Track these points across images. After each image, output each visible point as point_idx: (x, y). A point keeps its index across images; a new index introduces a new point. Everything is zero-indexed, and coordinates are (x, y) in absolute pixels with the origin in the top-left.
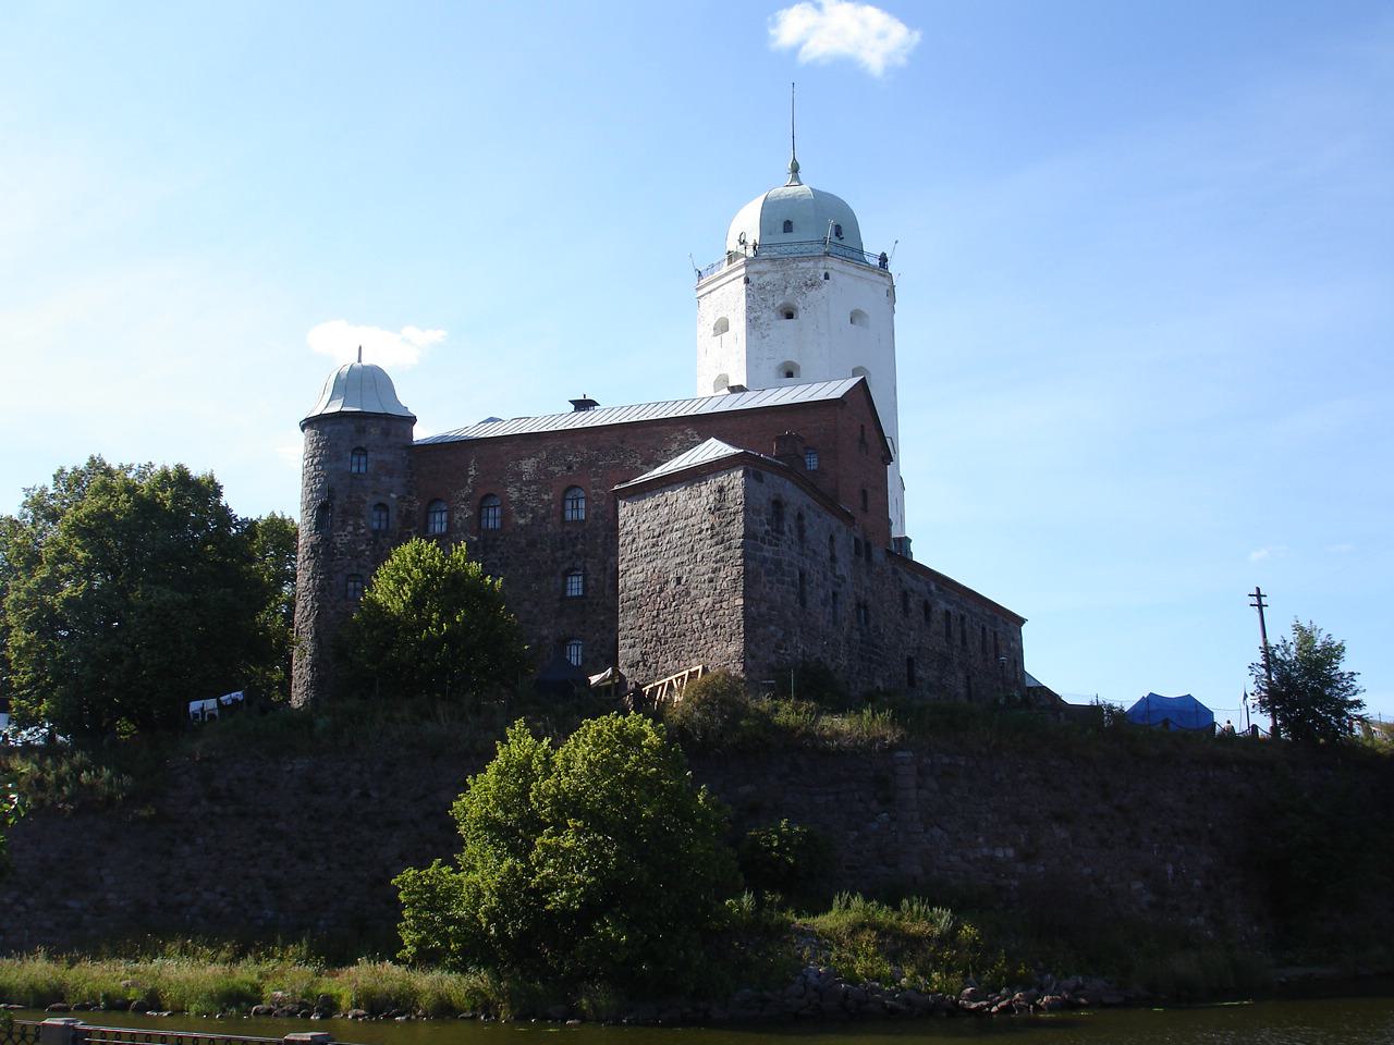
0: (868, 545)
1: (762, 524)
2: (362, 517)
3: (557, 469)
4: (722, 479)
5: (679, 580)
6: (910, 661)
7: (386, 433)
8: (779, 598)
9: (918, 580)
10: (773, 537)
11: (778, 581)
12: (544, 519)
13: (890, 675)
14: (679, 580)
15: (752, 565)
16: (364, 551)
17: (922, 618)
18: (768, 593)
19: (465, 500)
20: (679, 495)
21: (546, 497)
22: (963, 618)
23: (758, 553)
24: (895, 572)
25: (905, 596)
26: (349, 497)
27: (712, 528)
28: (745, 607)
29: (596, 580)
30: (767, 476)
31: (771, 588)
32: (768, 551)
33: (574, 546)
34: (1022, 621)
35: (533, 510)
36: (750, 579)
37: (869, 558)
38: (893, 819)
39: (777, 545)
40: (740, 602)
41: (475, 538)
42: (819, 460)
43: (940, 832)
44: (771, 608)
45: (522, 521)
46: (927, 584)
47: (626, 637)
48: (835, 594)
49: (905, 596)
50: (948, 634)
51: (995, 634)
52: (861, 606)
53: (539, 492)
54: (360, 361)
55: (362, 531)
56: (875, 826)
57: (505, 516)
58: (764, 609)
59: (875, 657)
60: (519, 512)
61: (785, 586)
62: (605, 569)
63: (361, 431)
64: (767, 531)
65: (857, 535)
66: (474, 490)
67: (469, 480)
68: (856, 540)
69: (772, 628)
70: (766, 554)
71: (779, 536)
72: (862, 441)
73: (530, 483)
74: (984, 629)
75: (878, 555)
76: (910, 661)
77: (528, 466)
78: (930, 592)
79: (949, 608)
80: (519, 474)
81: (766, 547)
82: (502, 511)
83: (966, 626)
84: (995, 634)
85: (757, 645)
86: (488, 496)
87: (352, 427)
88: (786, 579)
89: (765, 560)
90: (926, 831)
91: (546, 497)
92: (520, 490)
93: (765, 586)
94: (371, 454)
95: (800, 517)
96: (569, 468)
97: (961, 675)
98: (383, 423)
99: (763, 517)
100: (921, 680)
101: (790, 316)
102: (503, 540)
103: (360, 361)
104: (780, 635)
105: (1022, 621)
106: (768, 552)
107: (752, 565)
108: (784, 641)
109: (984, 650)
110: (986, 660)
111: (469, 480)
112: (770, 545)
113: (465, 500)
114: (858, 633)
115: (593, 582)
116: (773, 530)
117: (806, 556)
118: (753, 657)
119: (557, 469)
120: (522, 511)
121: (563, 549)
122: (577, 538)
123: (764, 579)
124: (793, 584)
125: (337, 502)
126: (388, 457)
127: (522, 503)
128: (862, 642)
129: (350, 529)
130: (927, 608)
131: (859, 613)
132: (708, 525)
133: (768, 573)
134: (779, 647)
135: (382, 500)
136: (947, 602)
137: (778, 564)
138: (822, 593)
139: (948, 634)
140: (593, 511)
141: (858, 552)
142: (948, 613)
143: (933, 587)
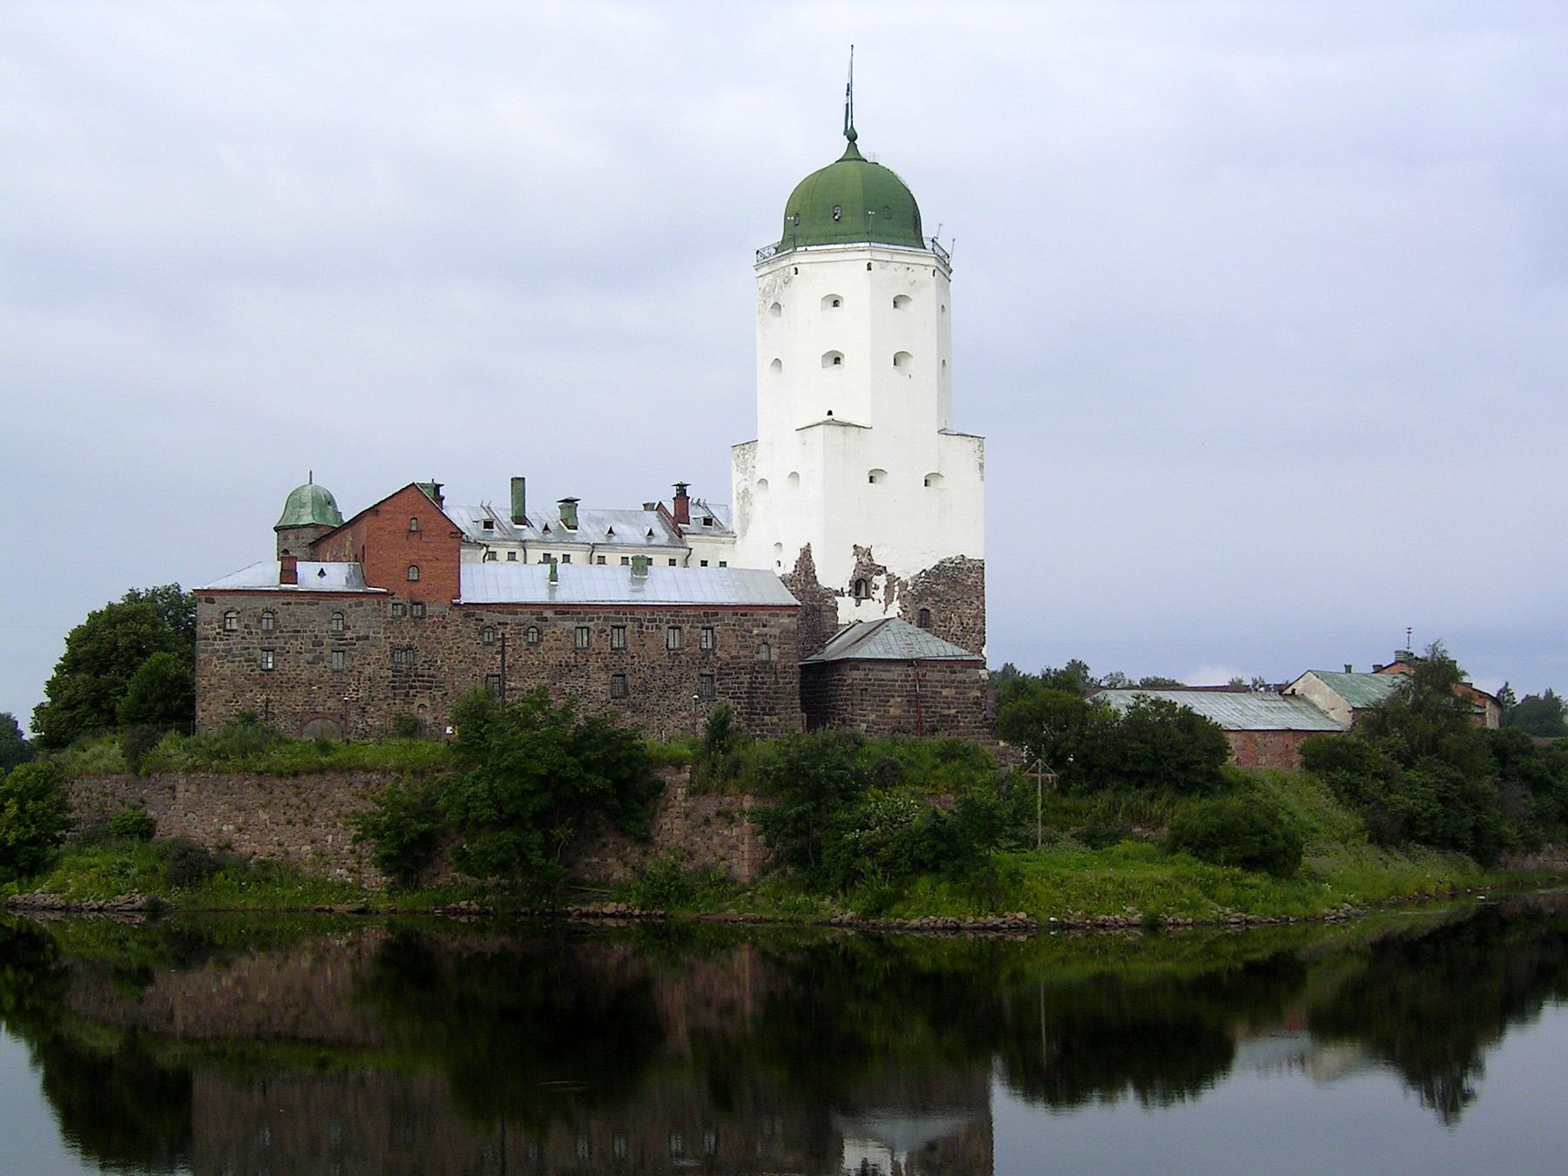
1: (215, 629)
8: (228, 672)
10: (224, 635)
11: (228, 661)
13: (446, 694)
18: (218, 671)
23: (209, 648)
32: (220, 645)
39: (227, 640)
43: (194, 815)
54: (311, 483)
59: (417, 684)
61: (237, 663)
63: (286, 539)
64: (218, 634)
69: (221, 691)
70: (218, 647)
71: (230, 633)
78: (545, 619)
79: (591, 625)
81: (218, 642)
83: (627, 633)
88: (237, 659)
93: (216, 666)
98: (295, 531)
100: (511, 690)
103: (311, 483)
104: (230, 694)
106: (219, 645)
108: (235, 697)
112: (221, 639)
116: (224, 631)
117: (276, 638)
118: (203, 711)
123: (215, 661)
128: (394, 676)
136: (579, 620)
138: (309, 657)
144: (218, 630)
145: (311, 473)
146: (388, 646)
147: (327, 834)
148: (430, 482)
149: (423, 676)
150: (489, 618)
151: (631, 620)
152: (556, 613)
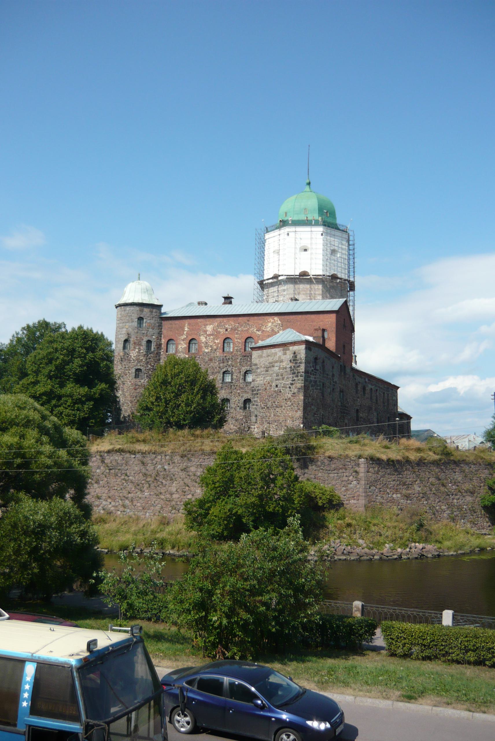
0: (345, 367)
1: (311, 367)
2: (142, 346)
3: (221, 330)
4: (295, 348)
5: (277, 386)
6: (357, 411)
7: (152, 312)
9: (361, 378)
12: (215, 350)
14: (277, 386)
15: (307, 383)
16: (142, 360)
17: (362, 393)
19: (183, 340)
20: (278, 351)
21: (216, 341)
22: (377, 390)
24: (354, 376)
25: (357, 385)
26: (137, 337)
27: (291, 367)
28: (304, 400)
29: (237, 376)
30: (313, 348)
31: (313, 392)
33: (228, 362)
34: (398, 388)
35: (211, 346)
36: (306, 389)
37: (345, 373)
38: (358, 484)
40: (303, 398)
41: (187, 356)
42: (328, 334)
44: (313, 399)
45: (206, 351)
46: (365, 379)
47: (254, 405)
48: (333, 389)
49: (357, 385)
50: (371, 398)
51: (388, 395)
52: (341, 391)
53: (214, 339)
55: (142, 351)
56: (352, 486)
57: (200, 347)
58: (310, 400)
60: (206, 347)
62: (240, 372)
63: (142, 311)
65: (341, 364)
66: (187, 337)
67: (185, 333)
68: (341, 366)
69: (313, 407)
70: (311, 379)
72: (344, 326)
73: (210, 335)
74: (384, 393)
75: (348, 370)
76: (357, 411)
77: (209, 328)
78: (366, 382)
79: (373, 387)
80: (205, 331)
81: (312, 376)
82: (199, 345)
84: (388, 395)
85: (308, 414)
86: (193, 339)
87: (138, 308)
89: (311, 381)
90: (370, 488)
91: (216, 341)
92: (206, 338)
94: (145, 321)
95: (323, 362)
96: (226, 330)
97: (375, 414)
99: (311, 365)
100: (361, 418)
101: (306, 250)
102: (199, 358)
105: (411, 418)
106: (312, 378)
107: (307, 383)
109: (384, 403)
110: (384, 406)
111: (185, 333)
112: (313, 375)
113: (183, 340)
114: (340, 404)
115: (235, 377)
118: (306, 418)
119: (221, 330)
120: (207, 347)
121: (223, 363)
122: (229, 359)
123: (311, 388)
124: (320, 389)
125: (131, 339)
126: (152, 321)
127: (207, 343)
129: (137, 350)
130: (364, 389)
131: (340, 394)
132: (289, 366)
133: (312, 386)
134: (315, 414)
135: (149, 338)
137: (315, 382)
139: (371, 398)
140: (236, 348)
141: (341, 371)
142: (371, 389)
143: (367, 380)
144: (312, 368)
145: (139, 275)
146: (339, 388)
147: (453, 499)
148: (226, 295)
149: (345, 407)
150: (358, 379)
151: (379, 387)
152: (369, 380)
